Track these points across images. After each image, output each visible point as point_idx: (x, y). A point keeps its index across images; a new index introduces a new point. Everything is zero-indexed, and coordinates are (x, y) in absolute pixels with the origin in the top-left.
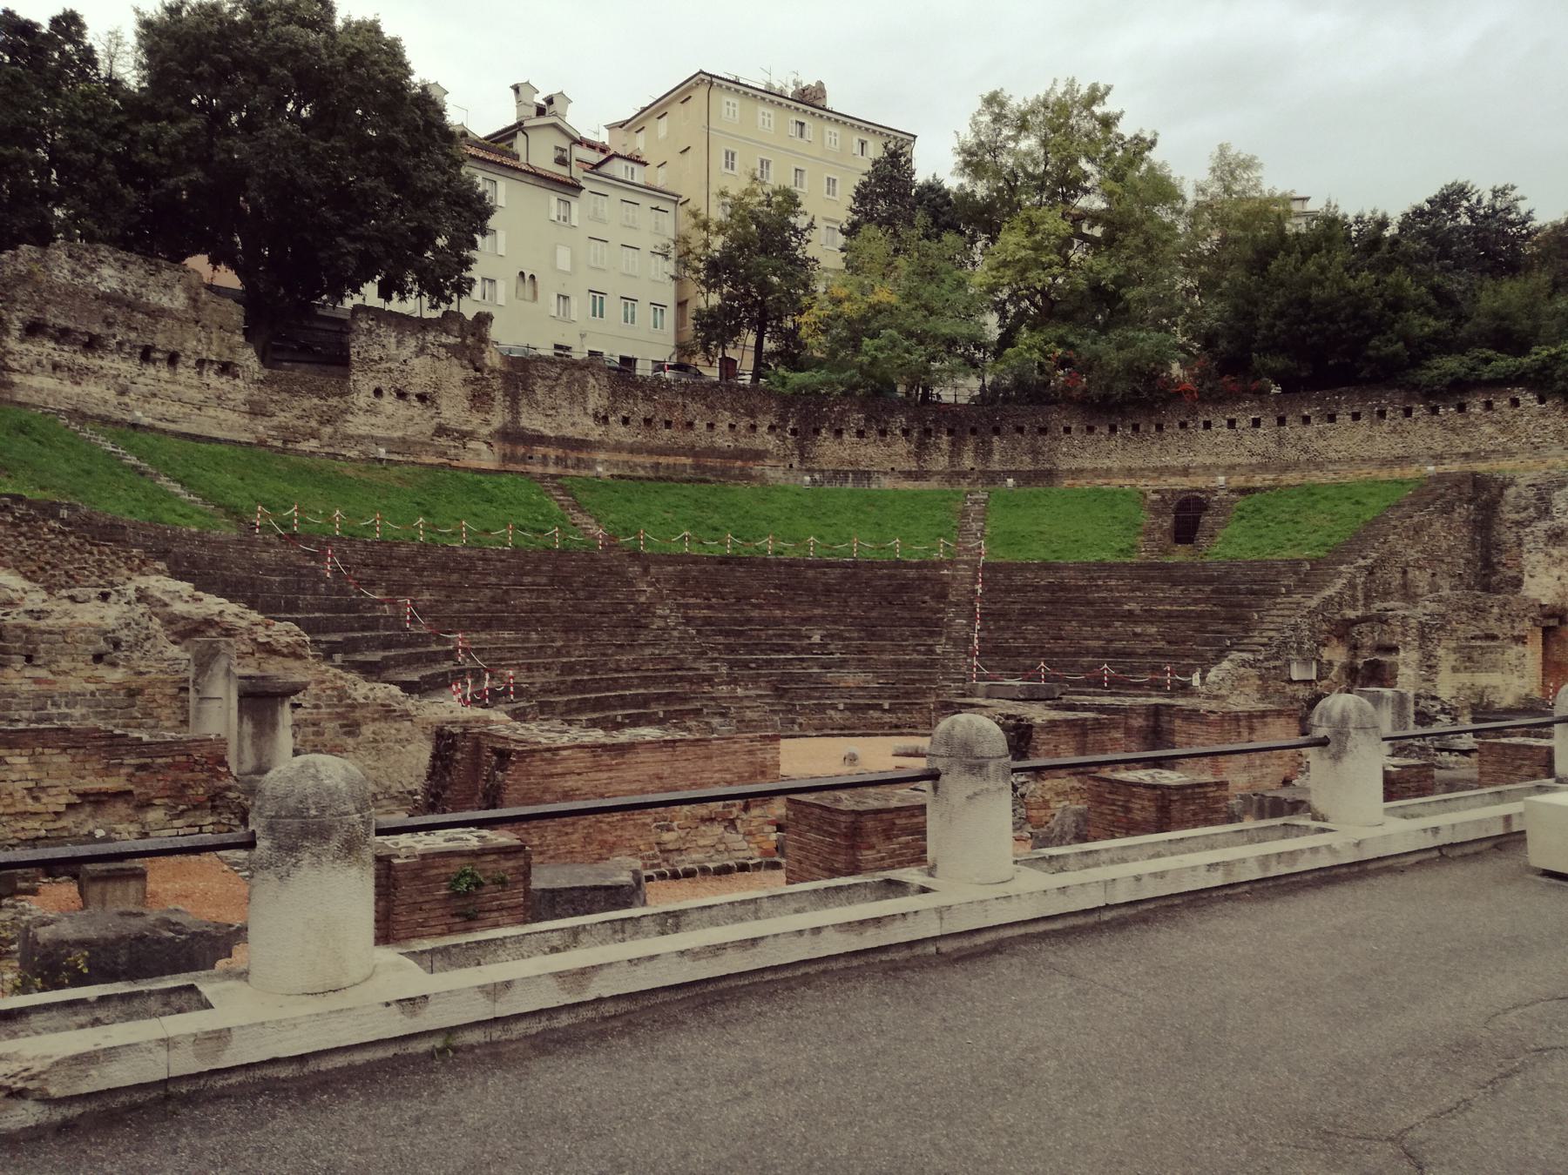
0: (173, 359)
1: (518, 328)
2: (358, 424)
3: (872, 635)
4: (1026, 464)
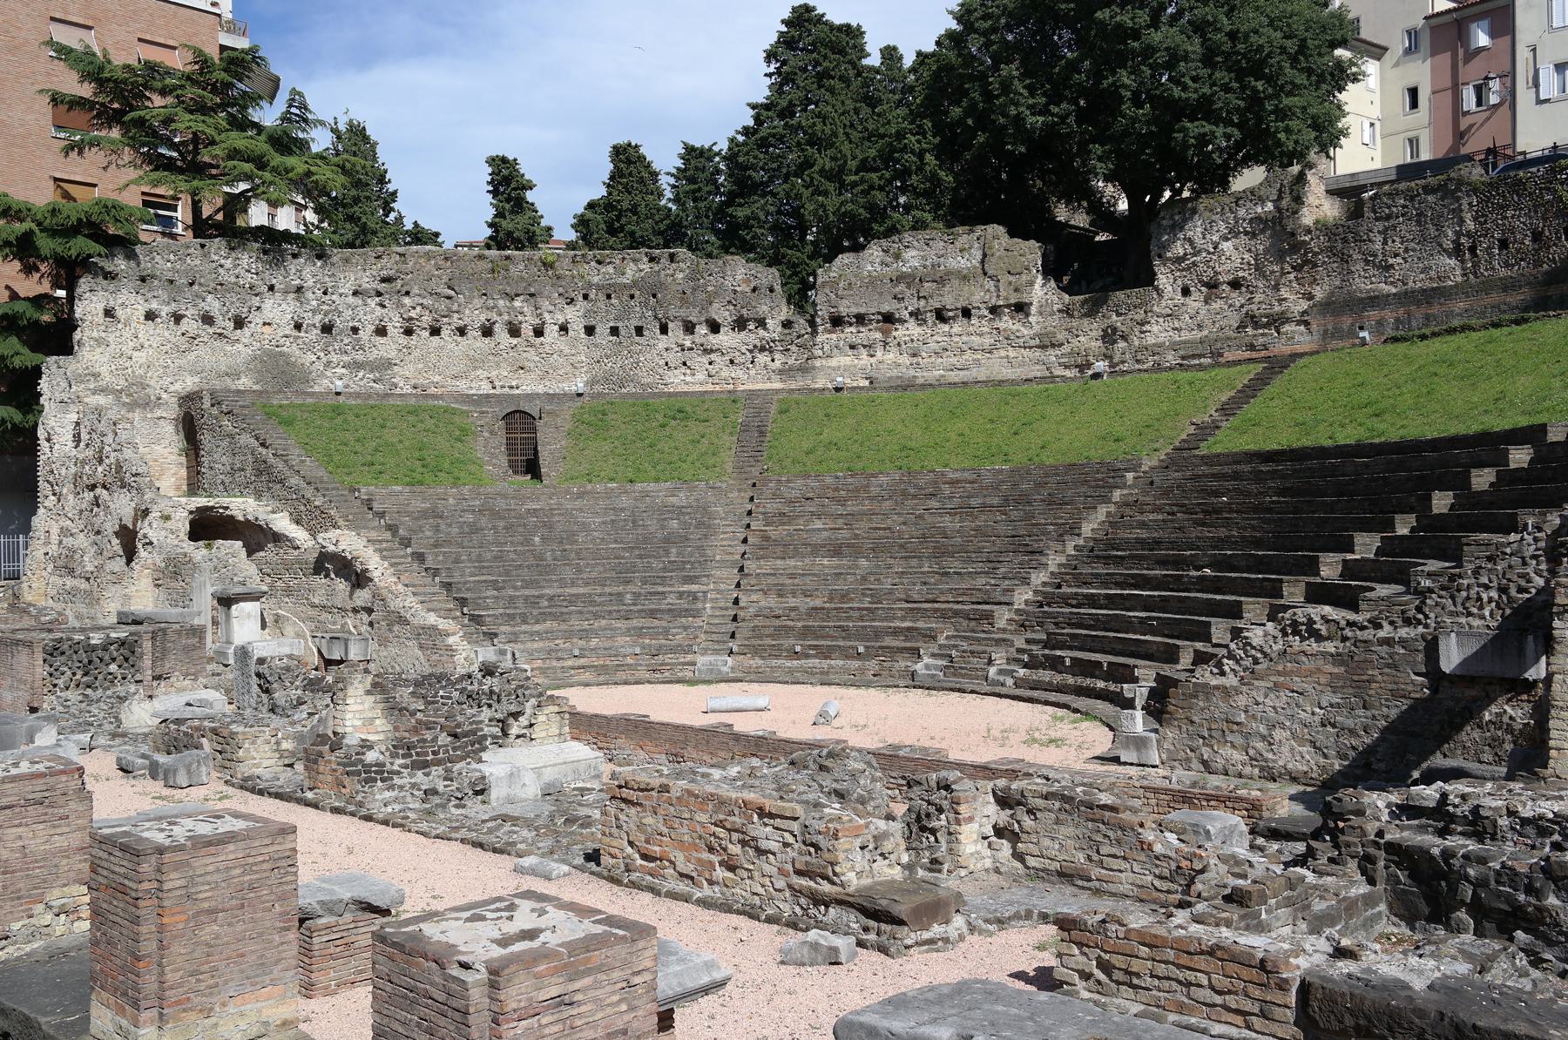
0: (967, 313)
2: (1158, 333)
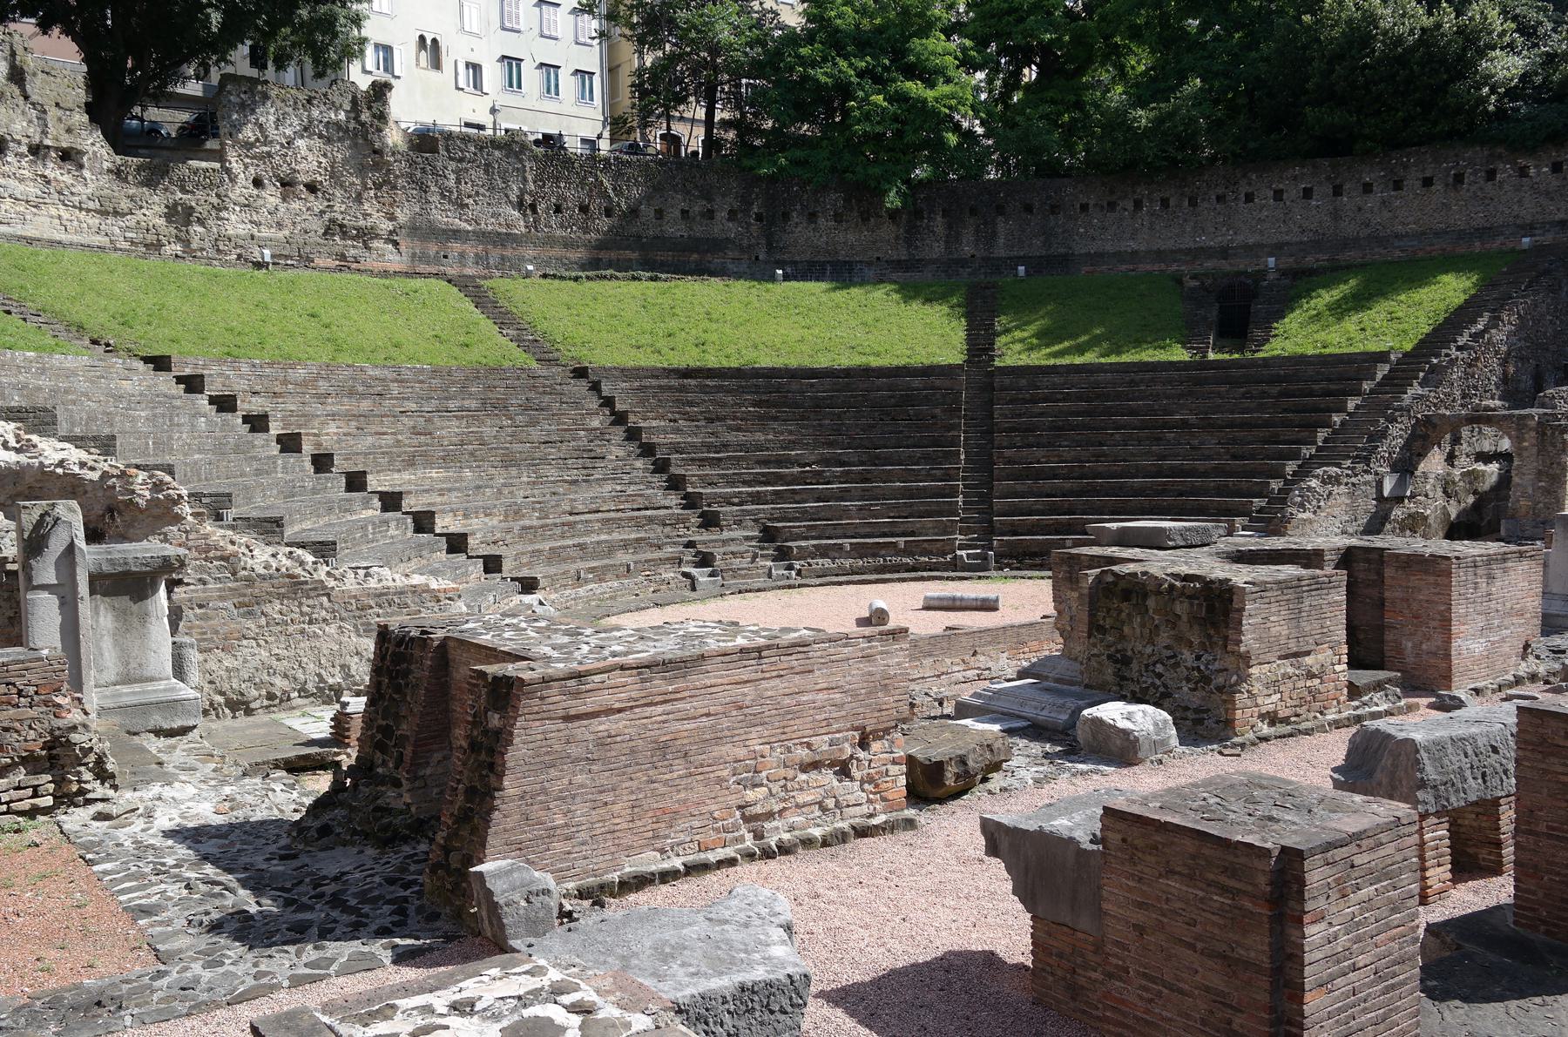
1: (417, 102)
3: (875, 460)
4: (1036, 247)
